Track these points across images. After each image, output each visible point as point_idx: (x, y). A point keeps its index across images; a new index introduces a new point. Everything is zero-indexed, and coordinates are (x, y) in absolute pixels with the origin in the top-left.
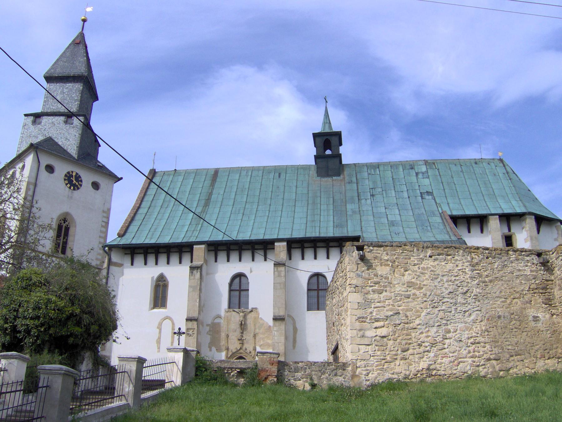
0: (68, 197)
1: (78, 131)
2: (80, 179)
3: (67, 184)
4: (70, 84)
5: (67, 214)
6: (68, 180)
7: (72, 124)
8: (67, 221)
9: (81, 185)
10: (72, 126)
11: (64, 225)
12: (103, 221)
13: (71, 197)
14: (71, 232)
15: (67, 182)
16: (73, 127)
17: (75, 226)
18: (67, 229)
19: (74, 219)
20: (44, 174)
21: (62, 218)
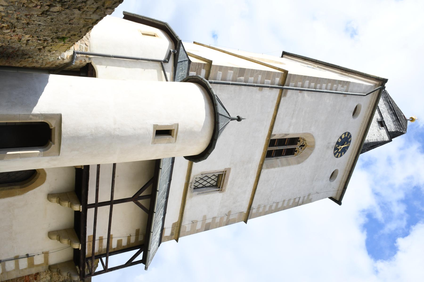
0: (329, 143)
1: (378, 137)
2: (343, 153)
3: (341, 137)
4: (390, 118)
5: (313, 147)
6: (345, 137)
7: (380, 129)
8: (301, 148)
9: (337, 157)
10: (379, 129)
11: (297, 147)
12: (300, 197)
13: (328, 148)
14: (290, 158)
15: (343, 137)
16: (378, 131)
17: (299, 163)
18: (291, 152)
19: (307, 158)
20: (352, 103)
21: (308, 140)
